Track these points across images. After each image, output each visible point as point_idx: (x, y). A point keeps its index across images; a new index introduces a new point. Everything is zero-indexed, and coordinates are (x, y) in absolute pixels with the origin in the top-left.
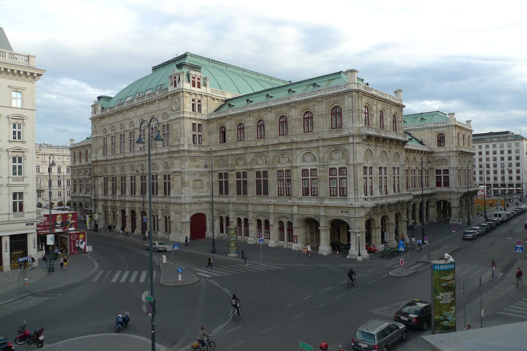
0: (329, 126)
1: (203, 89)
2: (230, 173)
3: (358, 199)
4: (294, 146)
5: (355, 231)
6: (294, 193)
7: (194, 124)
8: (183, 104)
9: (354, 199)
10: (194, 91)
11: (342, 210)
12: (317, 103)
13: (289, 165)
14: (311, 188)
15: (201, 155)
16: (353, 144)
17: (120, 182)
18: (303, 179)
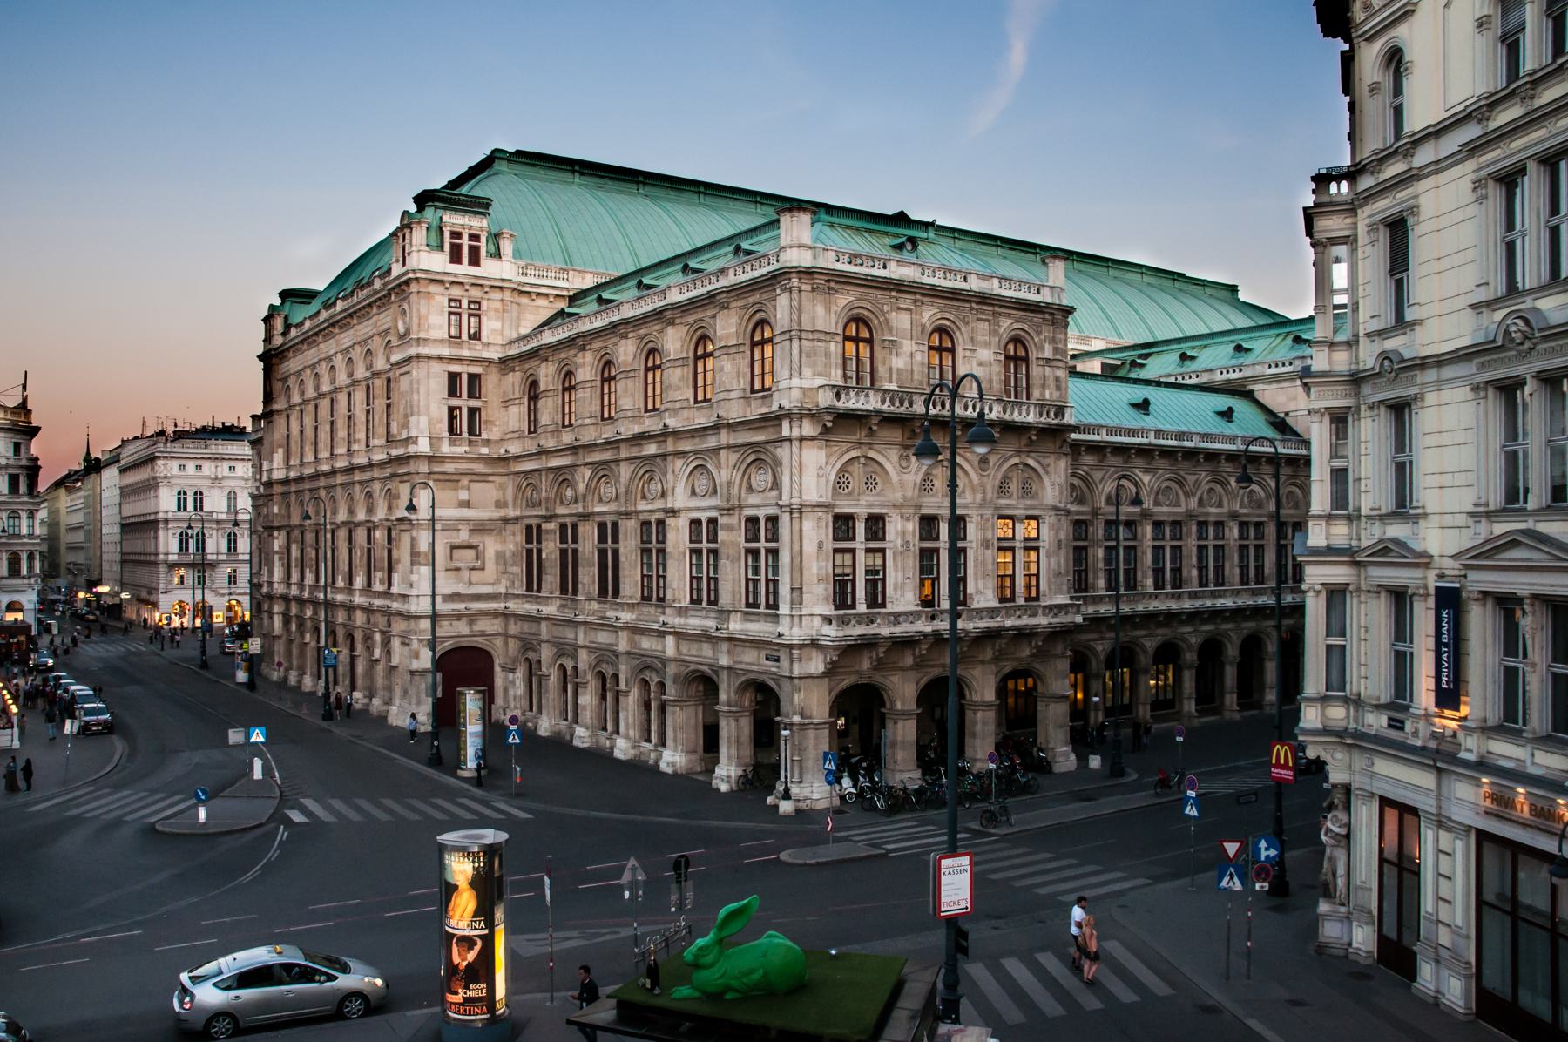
0: (744, 383)
1: (489, 268)
2: (544, 526)
3: (801, 621)
4: (670, 446)
5: (788, 720)
7: (453, 378)
9: (788, 619)
10: (456, 275)
11: (769, 652)
12: (717, 310)
13: (659, 504)
15: (479, 468)
16: (790, 440)
17: (311, 546)
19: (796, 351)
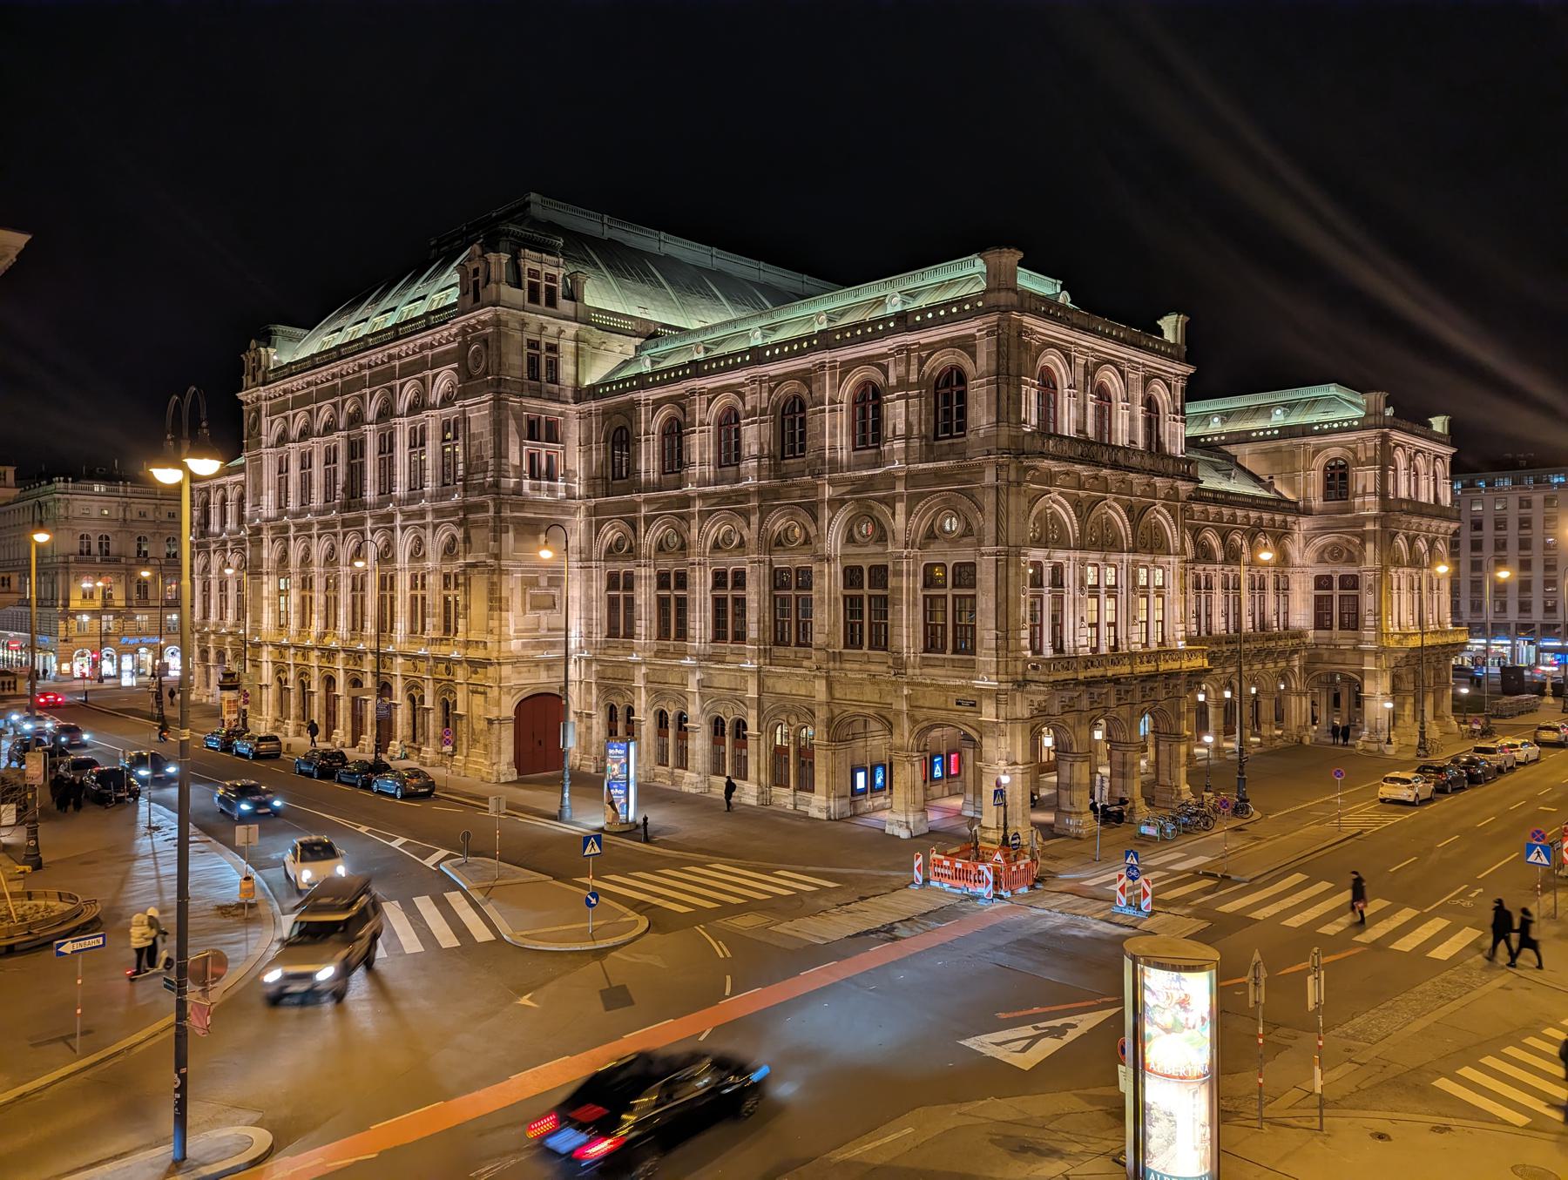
3: (1007, 666)
6: (818, 639)
8: (500, 356)
9: (994, 665)
11: (961, 695)
14: (871, 624)
18: (845, 597)
19: (1004, 397)
